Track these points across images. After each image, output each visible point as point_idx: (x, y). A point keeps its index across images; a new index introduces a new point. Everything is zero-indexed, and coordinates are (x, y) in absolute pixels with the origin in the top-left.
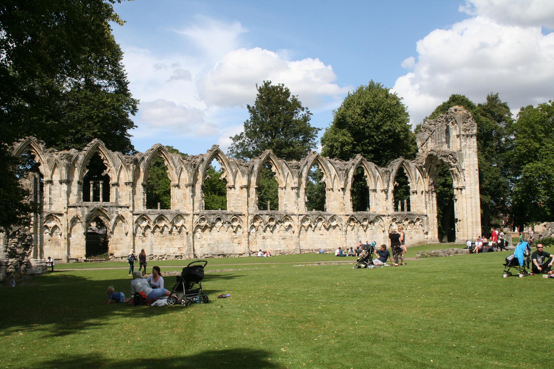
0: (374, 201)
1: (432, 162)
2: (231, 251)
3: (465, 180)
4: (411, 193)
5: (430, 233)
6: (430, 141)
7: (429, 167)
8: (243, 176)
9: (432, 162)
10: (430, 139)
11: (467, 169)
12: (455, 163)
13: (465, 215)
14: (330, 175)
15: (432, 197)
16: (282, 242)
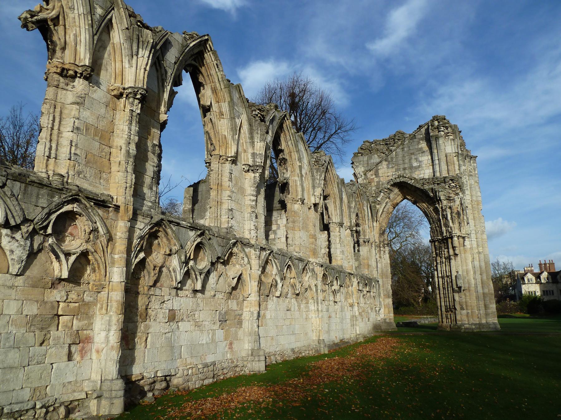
0: (338, 246)
1: (389, 198)
2: (26, 394)
3: (468, 223)
4: (361, 241)
5: (382, 310)
6: (385, 167)
7: (384, 205)
8: (133, 55)
9: (389, 198)
10: (384, 163)
11: (470, 206)
12: (457, 194)
13: (473, 282)
14: (300, 167)
15: (384, 252)
16: (220, 334)
